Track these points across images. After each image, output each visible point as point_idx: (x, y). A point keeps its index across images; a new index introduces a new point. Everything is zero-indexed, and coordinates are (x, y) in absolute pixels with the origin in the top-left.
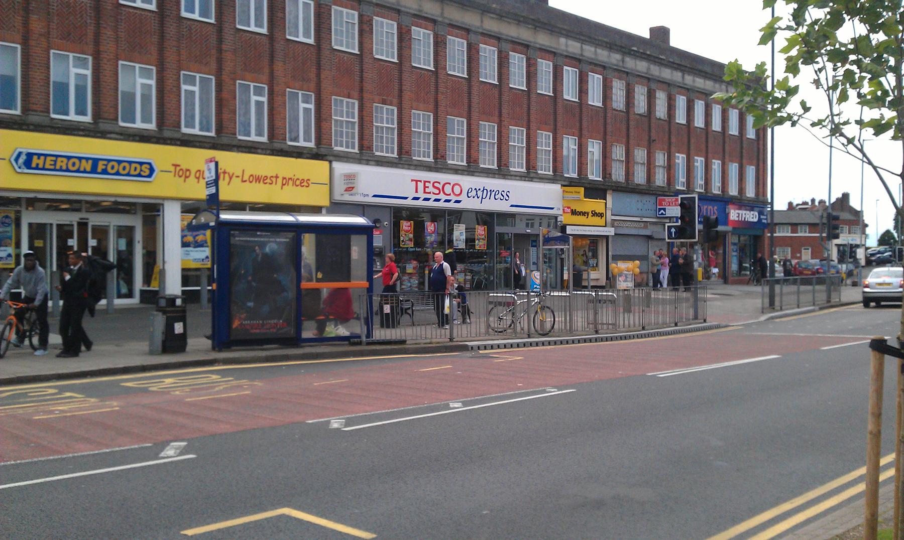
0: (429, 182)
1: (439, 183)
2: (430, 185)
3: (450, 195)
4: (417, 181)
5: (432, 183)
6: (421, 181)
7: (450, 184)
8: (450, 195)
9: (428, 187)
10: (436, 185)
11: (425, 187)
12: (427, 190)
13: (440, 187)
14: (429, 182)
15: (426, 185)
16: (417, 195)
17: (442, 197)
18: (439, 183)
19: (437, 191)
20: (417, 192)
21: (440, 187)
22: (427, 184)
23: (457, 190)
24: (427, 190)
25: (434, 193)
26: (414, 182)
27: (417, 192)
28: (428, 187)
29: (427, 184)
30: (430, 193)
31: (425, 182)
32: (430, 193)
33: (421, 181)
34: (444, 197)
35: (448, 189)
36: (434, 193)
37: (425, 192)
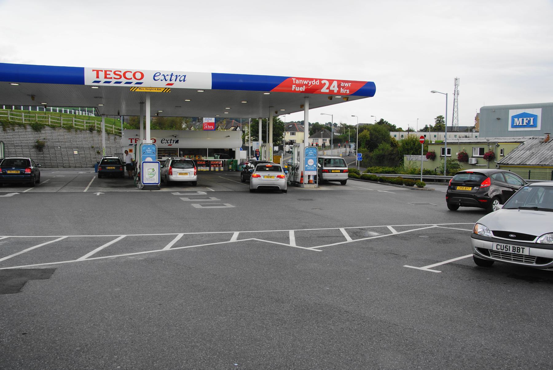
0: (111, 71)
1: (121, 72)
3: (131, 79)
4: (98, 72)
5: (113, 72)
6: (102, 71)
7: (131, 72)
8: (131, 79)
9: (110, 74)
10: (117, 73)
11: (106, 74)
13: (122, 74)
14: (111, 71)
16: (98, 80)
18: (121, 72)
19: (118, 77)
20: (98, 77)
21: (122, 74)
23: (138, 76)
24: (108, 76)
25: (114, 78)
26: (95, 72)
27: (98, 77)
28: (110, 74)
29: (108, 73)
30: (111, 78)
31: (106, 71)
32: (111, 78)
33: (102, 71)
36: (114, 78)
37: (106, 77)
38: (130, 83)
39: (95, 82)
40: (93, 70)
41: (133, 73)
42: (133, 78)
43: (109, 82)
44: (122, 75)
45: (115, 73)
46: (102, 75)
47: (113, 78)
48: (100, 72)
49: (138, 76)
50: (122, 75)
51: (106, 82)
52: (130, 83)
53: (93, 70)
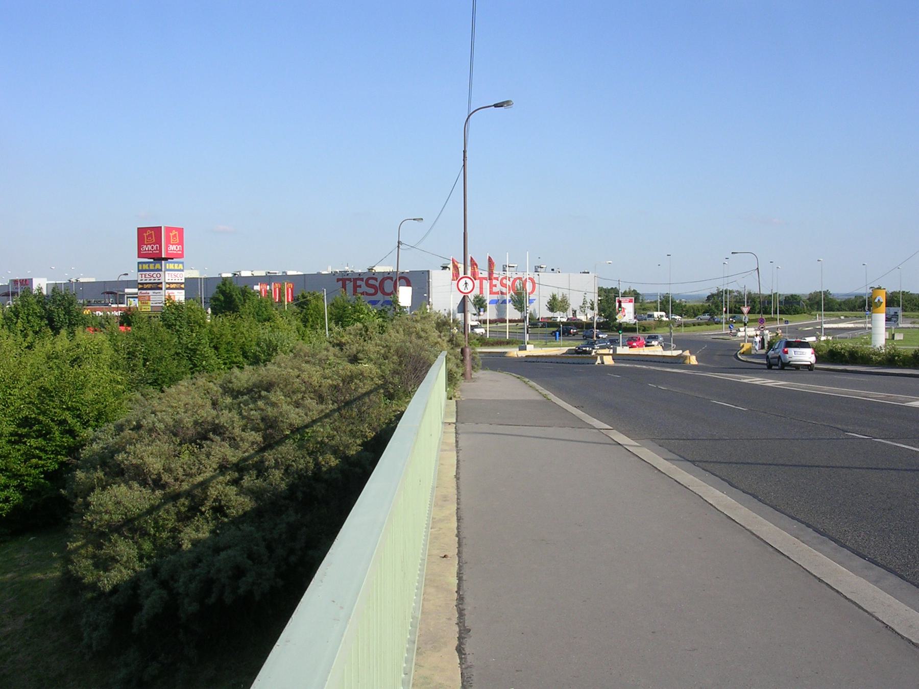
1: (376, 279)
2: (363, 284)
6: (349, 280)
10: (371, 282)
13: (377, 284)
14: (362, 280)
15: (358, 284)
18: (376, 279)
21: (377, 284)
22: (359, 283)
26: (341, 282)
28: (360, 286)
29: (359, 283)
31: (355, 280)
40: (338, 280)
44: (378, 286)
45: (368, 285)
48: (347, 282)
50: (378, 286)
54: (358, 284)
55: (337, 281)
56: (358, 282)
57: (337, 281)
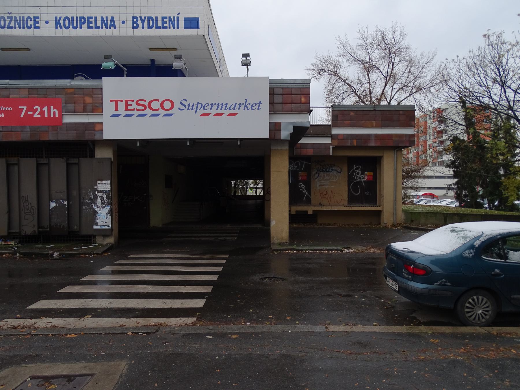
0: (133, 101)
1: (145, 101)
3: (158, 109)
4: (116, 102)
5: (135, 101)
6: (122, 101)
7: (158, 100)
8: (158, 109)
9: (131, 105)
10: (140, 102)
11: (127, 105)
12: (129, 107)
13: (146, 104)
14: (133, 101)
15: (128, 104)
17: (148, 111)
18: (145, 101)
19: (143, 108)
20: (117, 109)
21: (146, 104)
22: (129, 103)
23: (167, 105)
25: (137, 110)
26: (114, 102)
27: (117, 109)
28: (131, 105)
29: (129, 103)
30: (133, 110)
31: (126, 101)
32: (133, 110)
33: (122, 101)
34: (151, 112)
35: (156, 105)
36: (137, 110)
37: (126, 109)
38: (158, 115)
39: (114, 116)
40: (111, 101)
41: (160, 101)
42: (161, 109)
43: (131, 115)
44: (147, 105)
45: (137, 103)
46: (121, 105)
47: (135, 109)
48: (118, 102)
49: (167, 105)
50: (147, 105)
51: (127, 115)
52: (158, 115)
53: (111, 101)
54: (128, 104)
55: (110, 102)
56: (128, 102)
57: (110, 102)
